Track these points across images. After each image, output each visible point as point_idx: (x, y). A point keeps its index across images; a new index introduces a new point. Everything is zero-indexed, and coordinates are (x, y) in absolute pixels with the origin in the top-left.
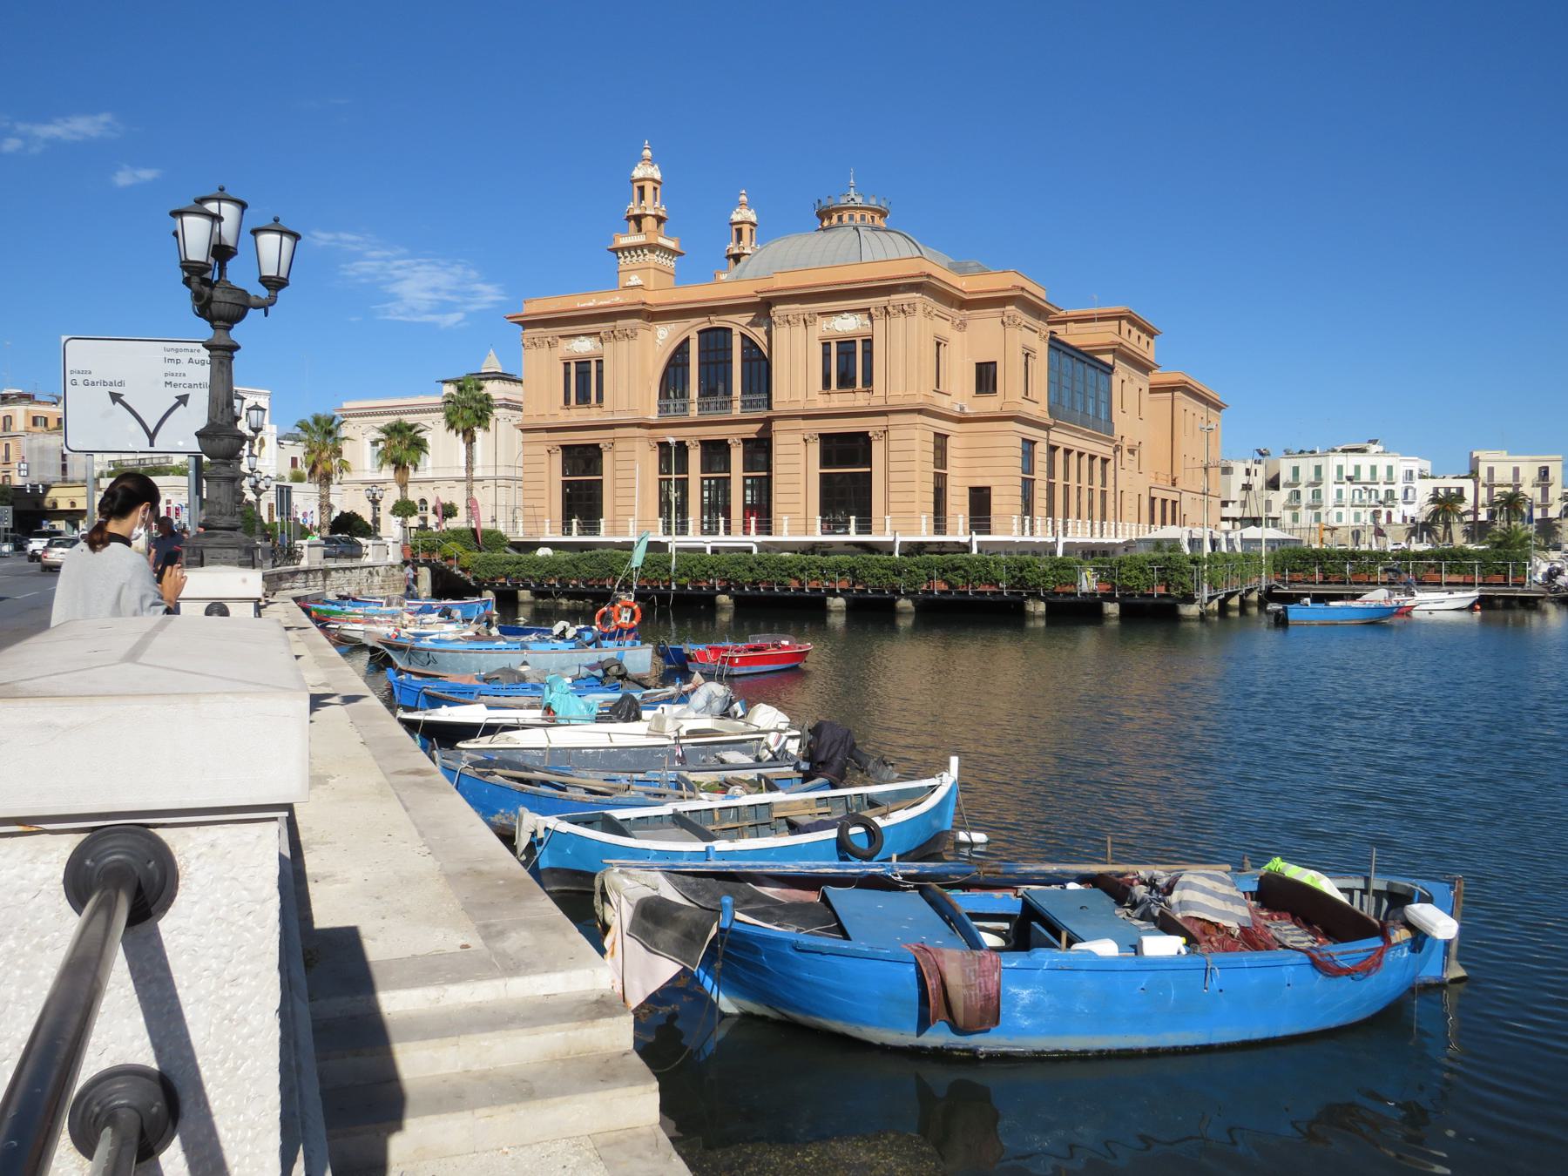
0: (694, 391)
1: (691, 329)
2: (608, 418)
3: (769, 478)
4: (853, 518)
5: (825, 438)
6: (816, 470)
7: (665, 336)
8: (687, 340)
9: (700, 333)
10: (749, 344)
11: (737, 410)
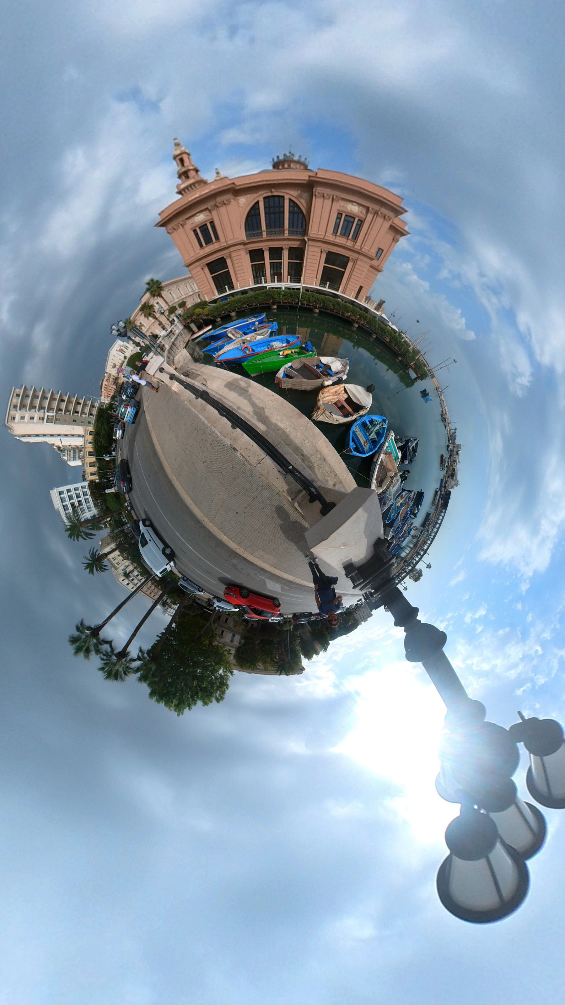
0: (264, 227)
1: (260, 197)
3: (301, 264)
5: (329, 254)
6: (322, 264)
7: (244, 203)
8: (258, 202)
9: (264, 198)
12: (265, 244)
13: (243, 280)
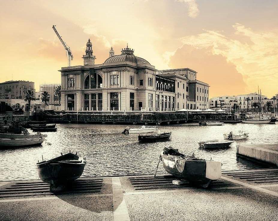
2: (75, 89)
4: (114, 108)
10: (99, 76)
11: (97, 88)
12: (90, 91)
13: (79, 107)
